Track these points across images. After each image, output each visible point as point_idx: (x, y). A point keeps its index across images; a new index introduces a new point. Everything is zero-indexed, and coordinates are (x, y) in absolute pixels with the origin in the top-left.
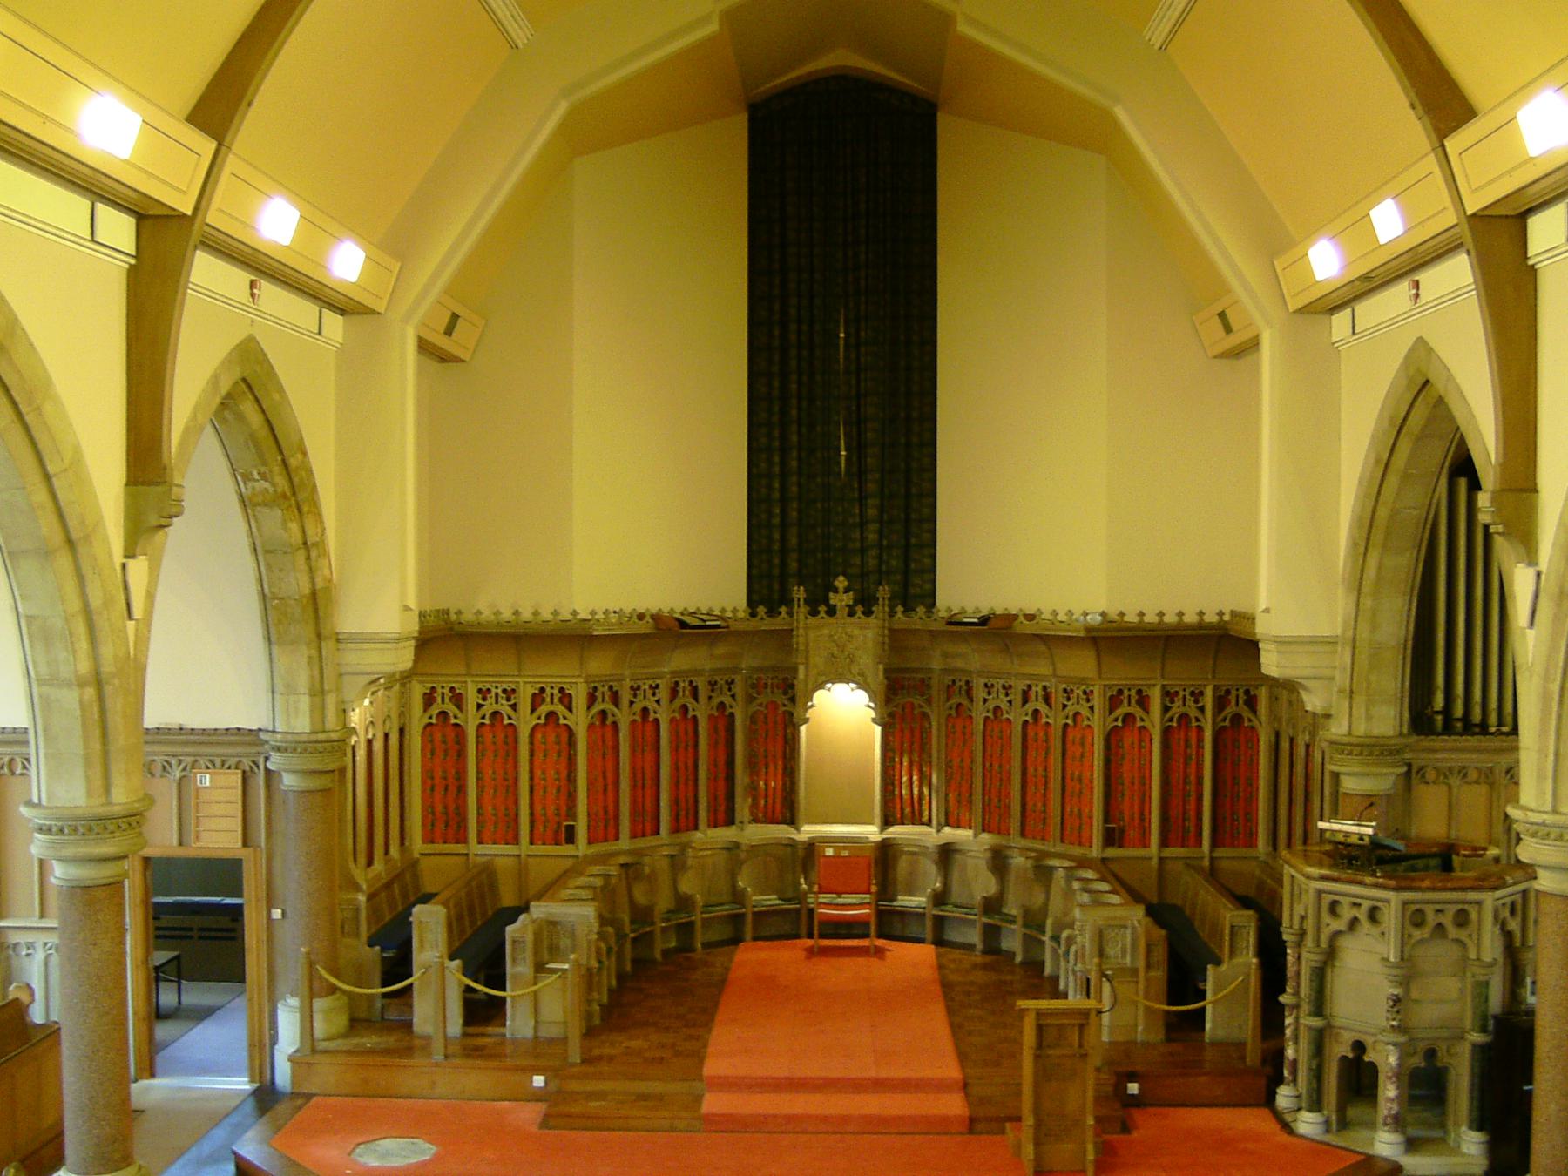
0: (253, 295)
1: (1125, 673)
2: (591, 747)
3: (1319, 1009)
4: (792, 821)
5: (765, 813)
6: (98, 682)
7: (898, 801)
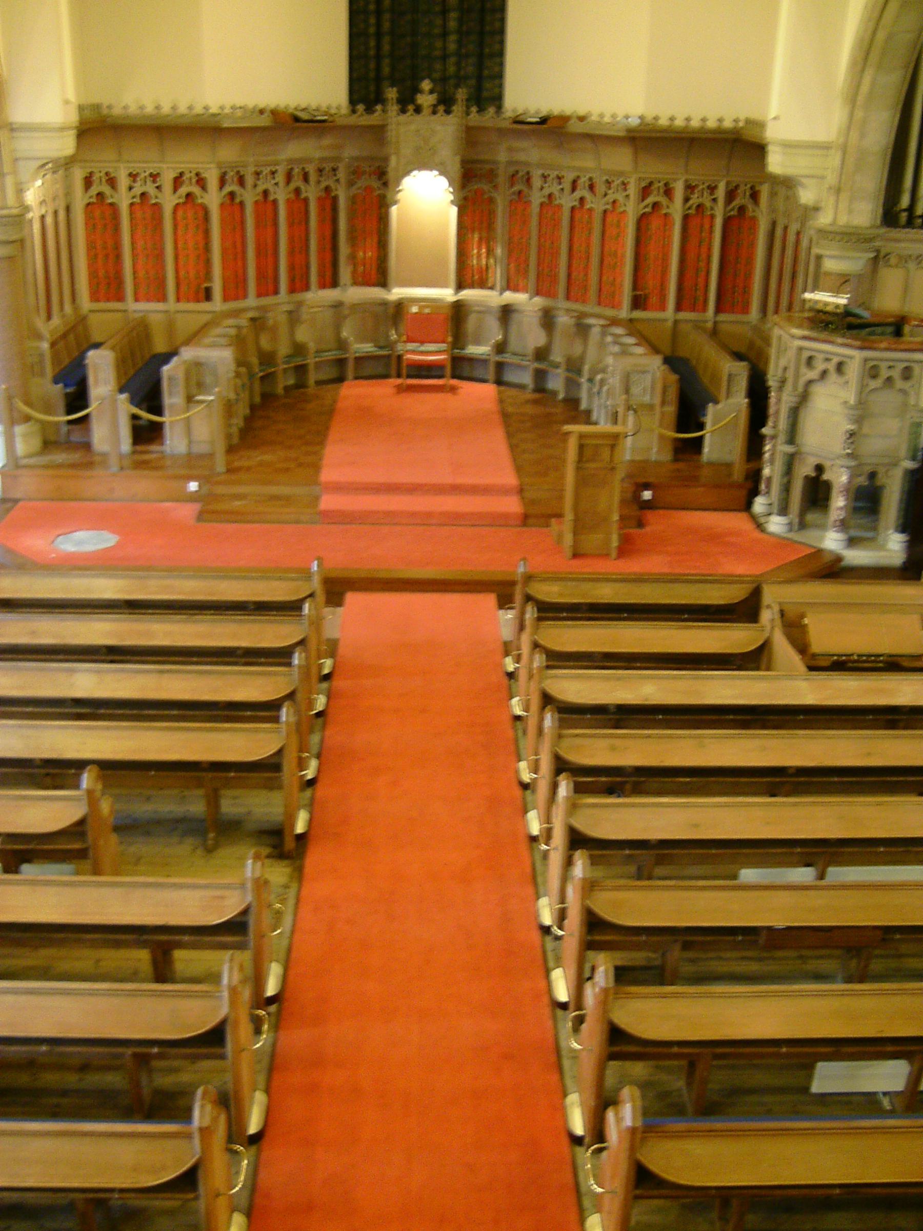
2: (223, 221)
3: (792, 439)
4: (383, 283)
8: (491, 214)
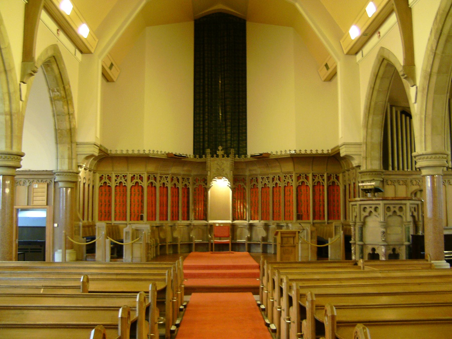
0: (58, 33)
1: (302, 169)
3: (362, 239)
4: (206, 220)
5: (198, 218)
6: (11, 115)
7: (237, 213)
8: (244, 194)
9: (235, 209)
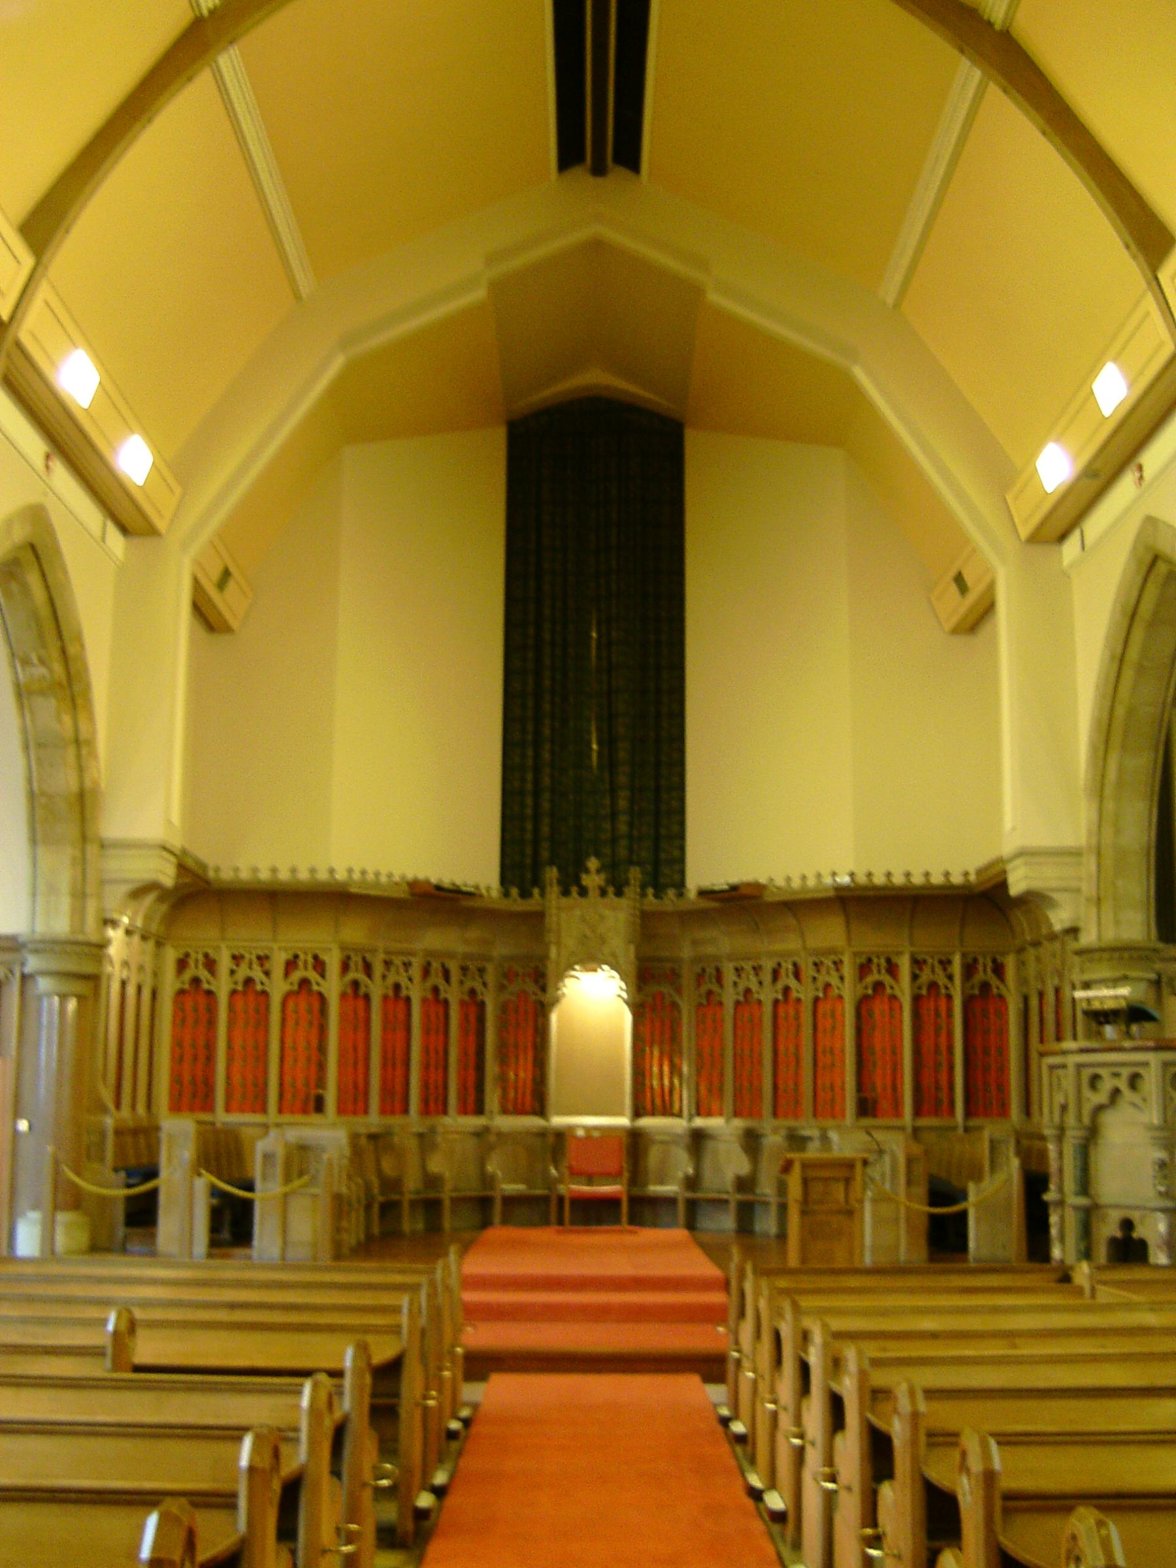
0: (47, 467)
2: (343, 1016)
3: (1085, 1185)
4: (541, 1110)
9: (644, 1075)
